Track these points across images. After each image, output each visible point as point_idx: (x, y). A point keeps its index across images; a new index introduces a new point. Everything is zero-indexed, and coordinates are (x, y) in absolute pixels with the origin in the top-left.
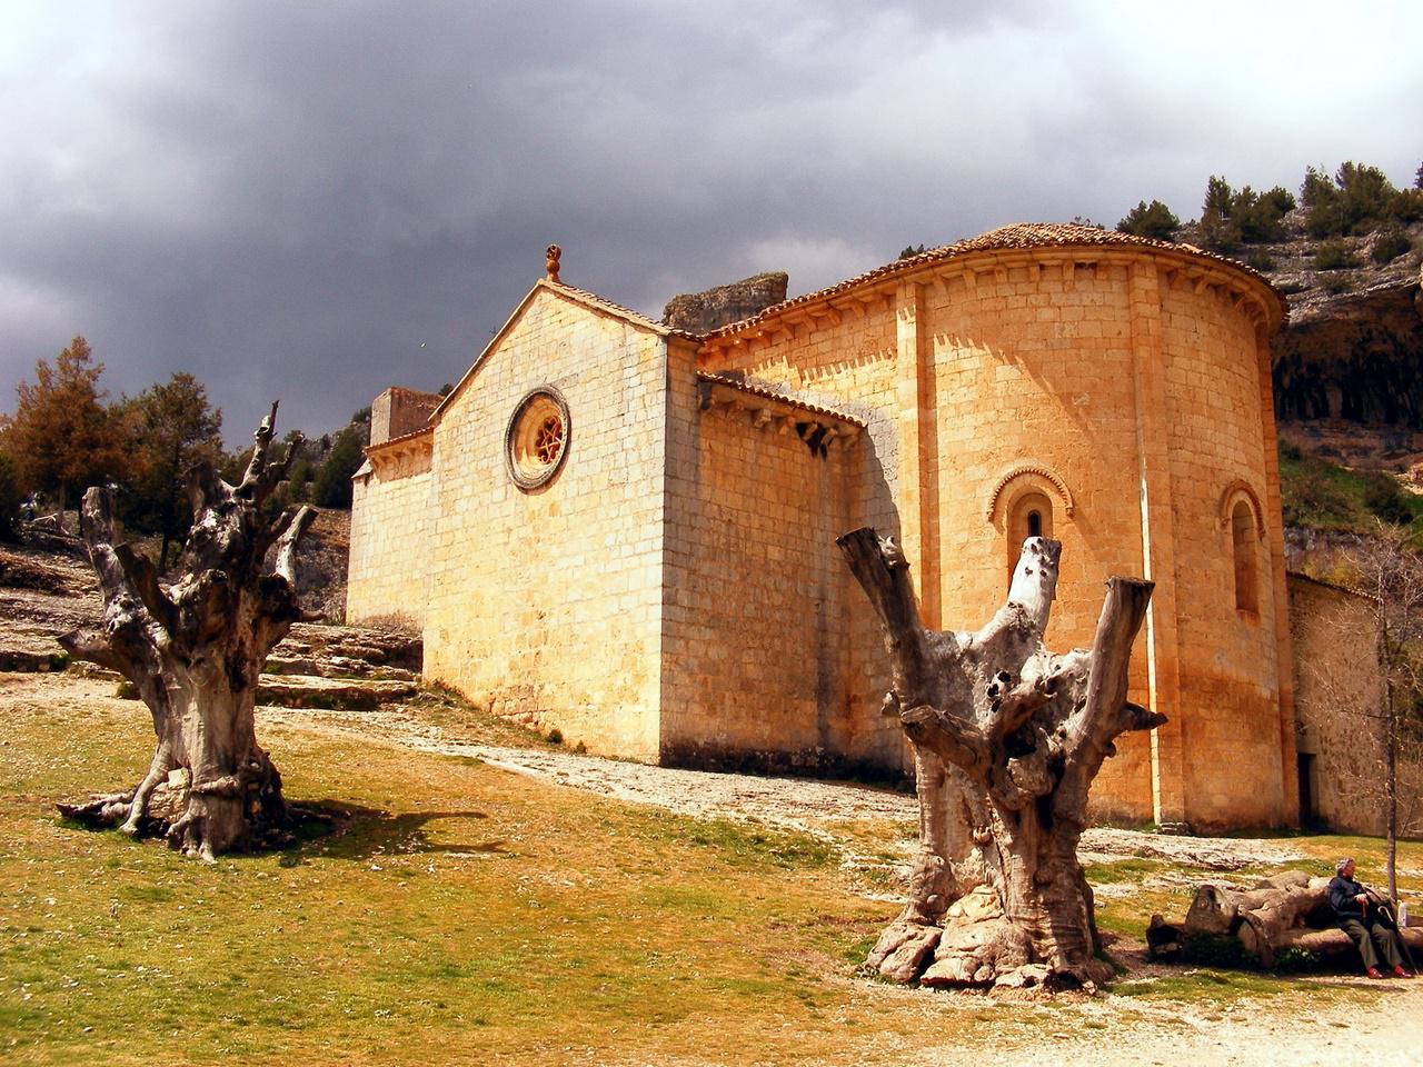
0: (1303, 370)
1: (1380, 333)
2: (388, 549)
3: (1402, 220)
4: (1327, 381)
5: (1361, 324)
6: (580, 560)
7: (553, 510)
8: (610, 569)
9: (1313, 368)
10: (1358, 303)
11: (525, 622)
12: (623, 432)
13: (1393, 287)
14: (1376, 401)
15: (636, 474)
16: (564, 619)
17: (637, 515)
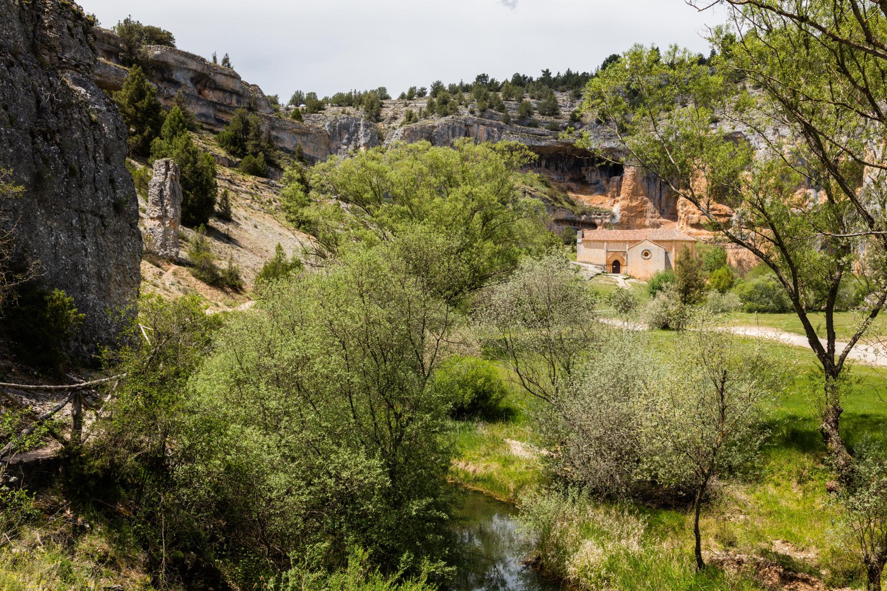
10: (562, 143)
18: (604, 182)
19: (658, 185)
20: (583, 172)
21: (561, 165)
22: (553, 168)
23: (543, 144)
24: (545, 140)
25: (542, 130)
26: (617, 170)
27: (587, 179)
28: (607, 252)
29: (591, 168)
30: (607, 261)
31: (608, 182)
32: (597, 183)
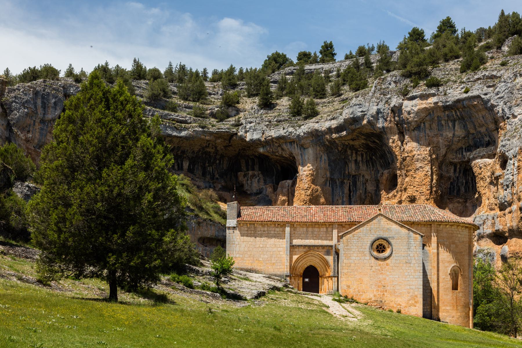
0: (179, 152)
1: (213, 145)
2: (246, 249)
3: (228, 105)
4: (185, 157)
5: (208, 141)
6: (397, 276)
7: (387, 265)
8: (406, 279)
9: (183, 152)
10: (211, 133)
11: (379, 287)
12: (409, 252)
13: (226, 132)
14: (200, 168)
15: (414, 262)
16: (392, 288)
17: (414, 270)
18: (270, 190)
19: (346, 191)
20: (241, 178)
21: (210, 169)
22: (199, 172)
23: (183, 134)
24: (185, 129)
25: (182, 115)
26: (289, 171)
27: (246, 187)
28: (293, 247)
29: (250, 173)
30: (292, 268)
31: (275, 189)
32: (260, 192)
